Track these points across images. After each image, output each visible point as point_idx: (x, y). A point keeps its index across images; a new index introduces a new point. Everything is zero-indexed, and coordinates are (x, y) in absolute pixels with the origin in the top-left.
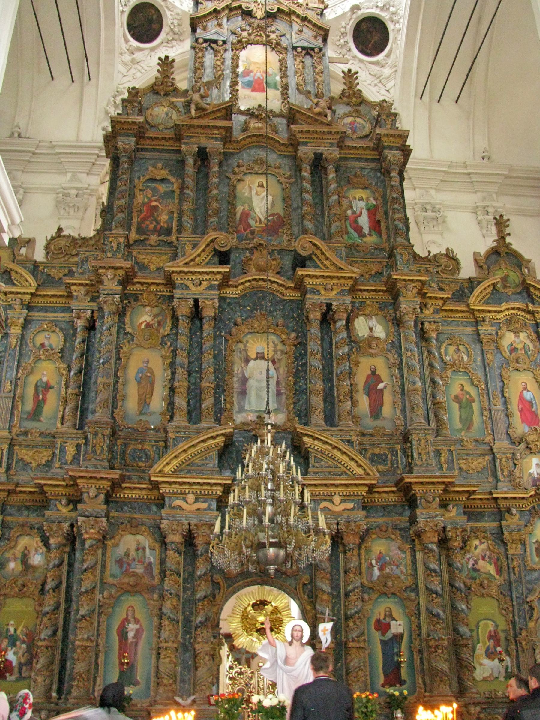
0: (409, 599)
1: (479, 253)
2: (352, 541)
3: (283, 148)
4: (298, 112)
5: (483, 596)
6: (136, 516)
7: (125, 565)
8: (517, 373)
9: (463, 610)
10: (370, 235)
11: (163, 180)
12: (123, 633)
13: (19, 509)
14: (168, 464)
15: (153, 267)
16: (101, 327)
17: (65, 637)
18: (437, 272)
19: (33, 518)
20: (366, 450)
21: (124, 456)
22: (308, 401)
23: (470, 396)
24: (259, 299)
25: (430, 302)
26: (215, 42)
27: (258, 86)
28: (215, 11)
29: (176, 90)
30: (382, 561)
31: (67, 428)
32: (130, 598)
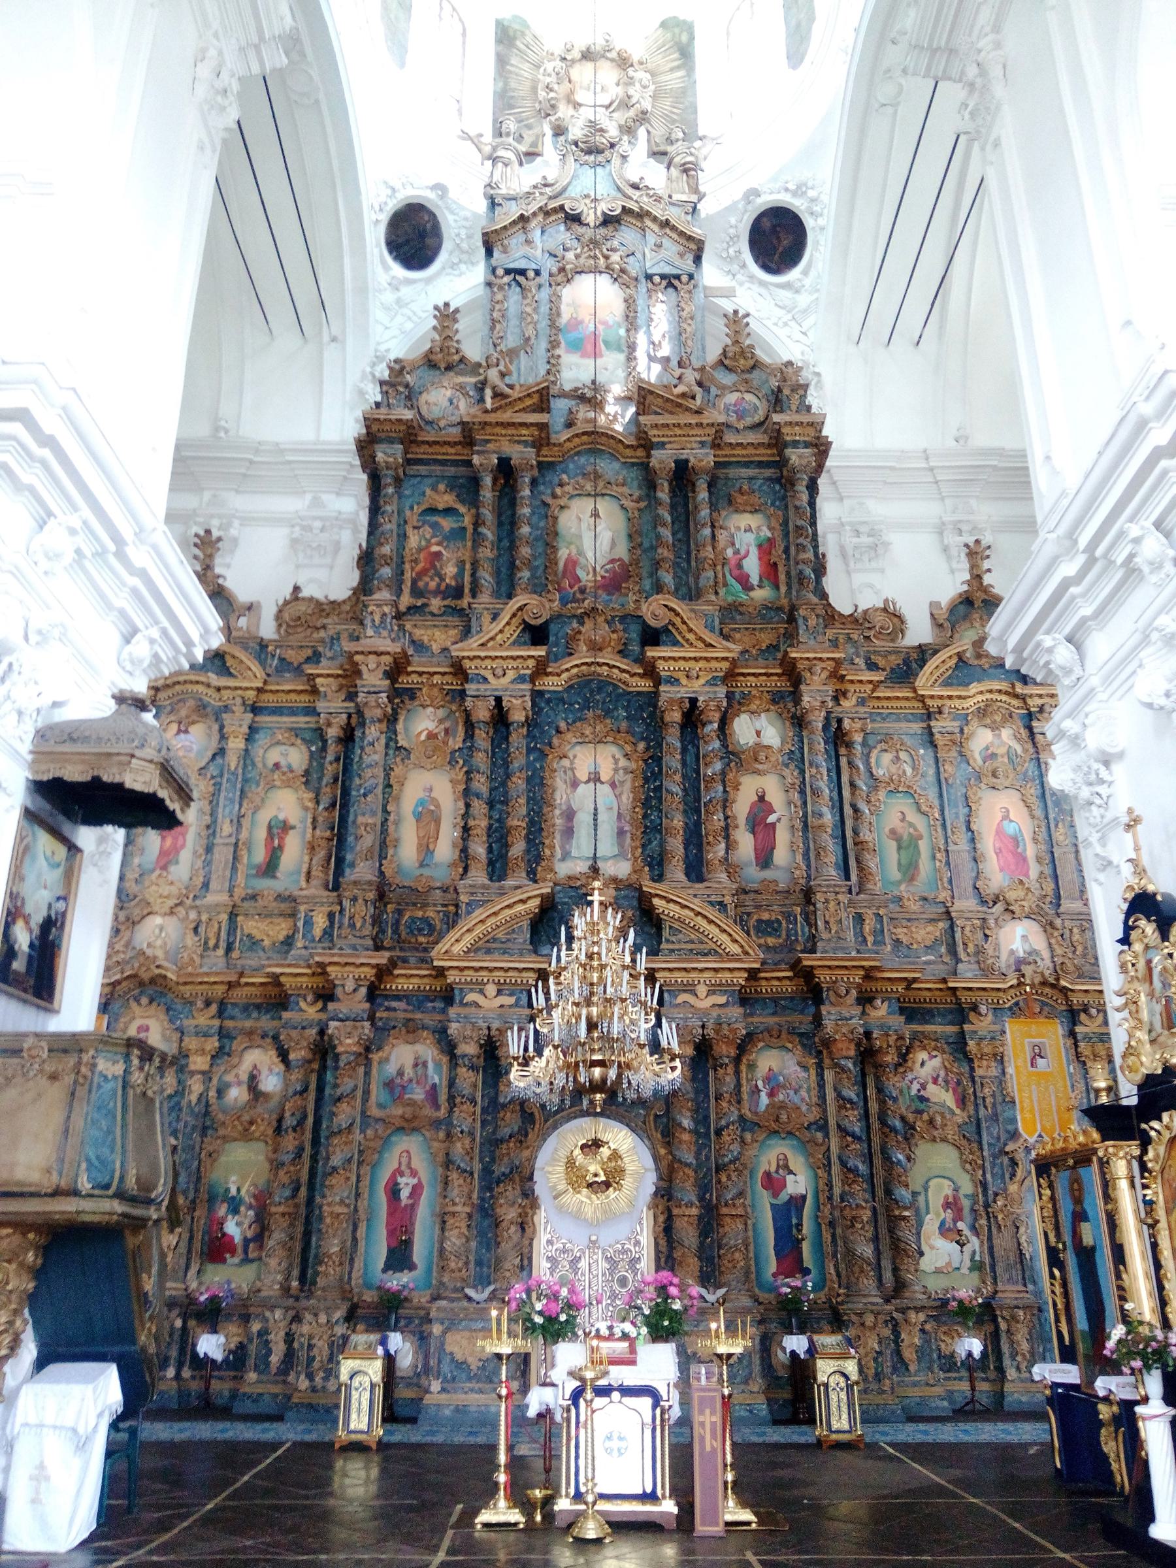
0: (812, 1141)
1: (938, 604)
3: (628, 452)
4: (652, 393)
5: (934, 1140)
7: (397, 1091)
10: (760, 586)
11: (449, 511)
12: (393, 1192)
15: (435, 648)
16: (362, 739)
17: (310, 1201)
19: (266, 1023)
22: (662, 844)
23: (916, 829)
25: (851, 688)
26: (522, 272)
30: (773, 1084)
31: (314, 889)
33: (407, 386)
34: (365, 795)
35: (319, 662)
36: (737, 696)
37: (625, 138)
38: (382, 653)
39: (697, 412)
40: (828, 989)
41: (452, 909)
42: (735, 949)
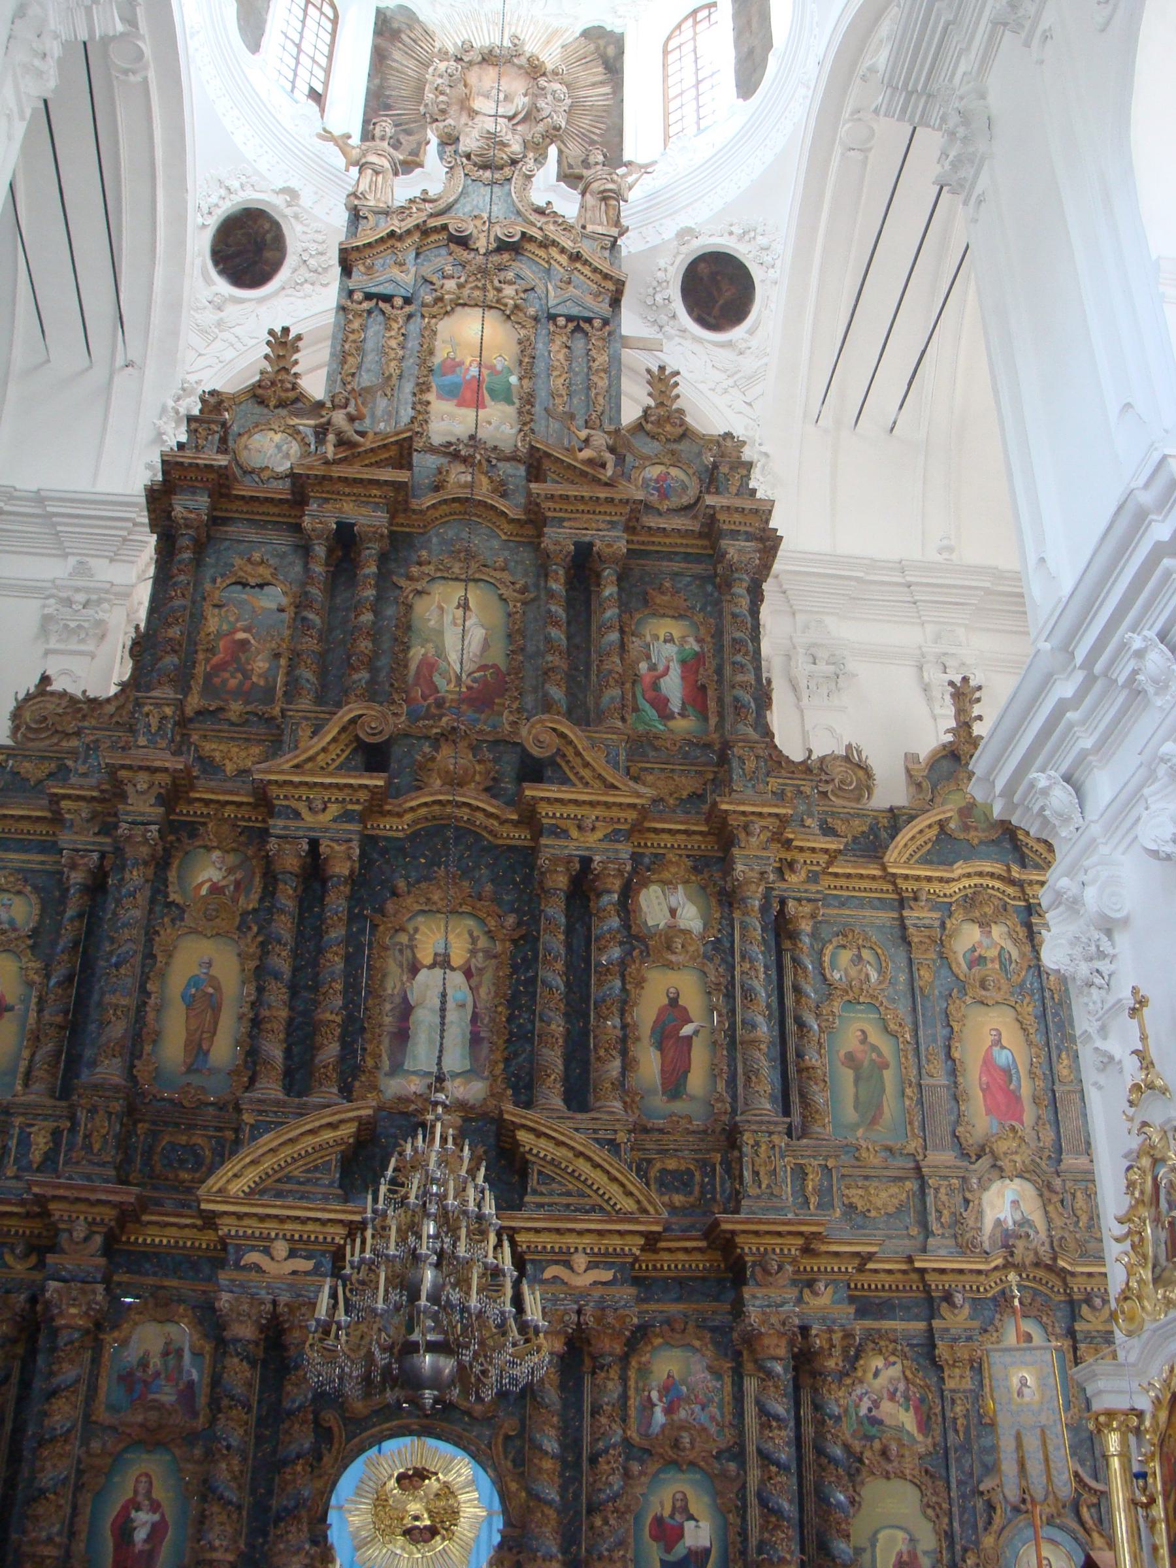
0: (724, 1474)
2: (607, 1348)
7: (139, 1387)
8: (984, 1009)
9: (839, 1503)
10: (683, 715)
20: (649, 1161)
23: (880, 1054)
25: (801, 858)
26: (387, 299)
27: (472, 395)
28: (392, 234)
29: (300, 397)
31: (37, 1094)
33: (224, 424)
34: (117, 966)
35: (66, 779)
36: (647, 860)
37: (531, 155)
38: (155, 770)
39: (606, 484)
40: (754, 1264)
41: (230, 1135)
42: (628, 1205)
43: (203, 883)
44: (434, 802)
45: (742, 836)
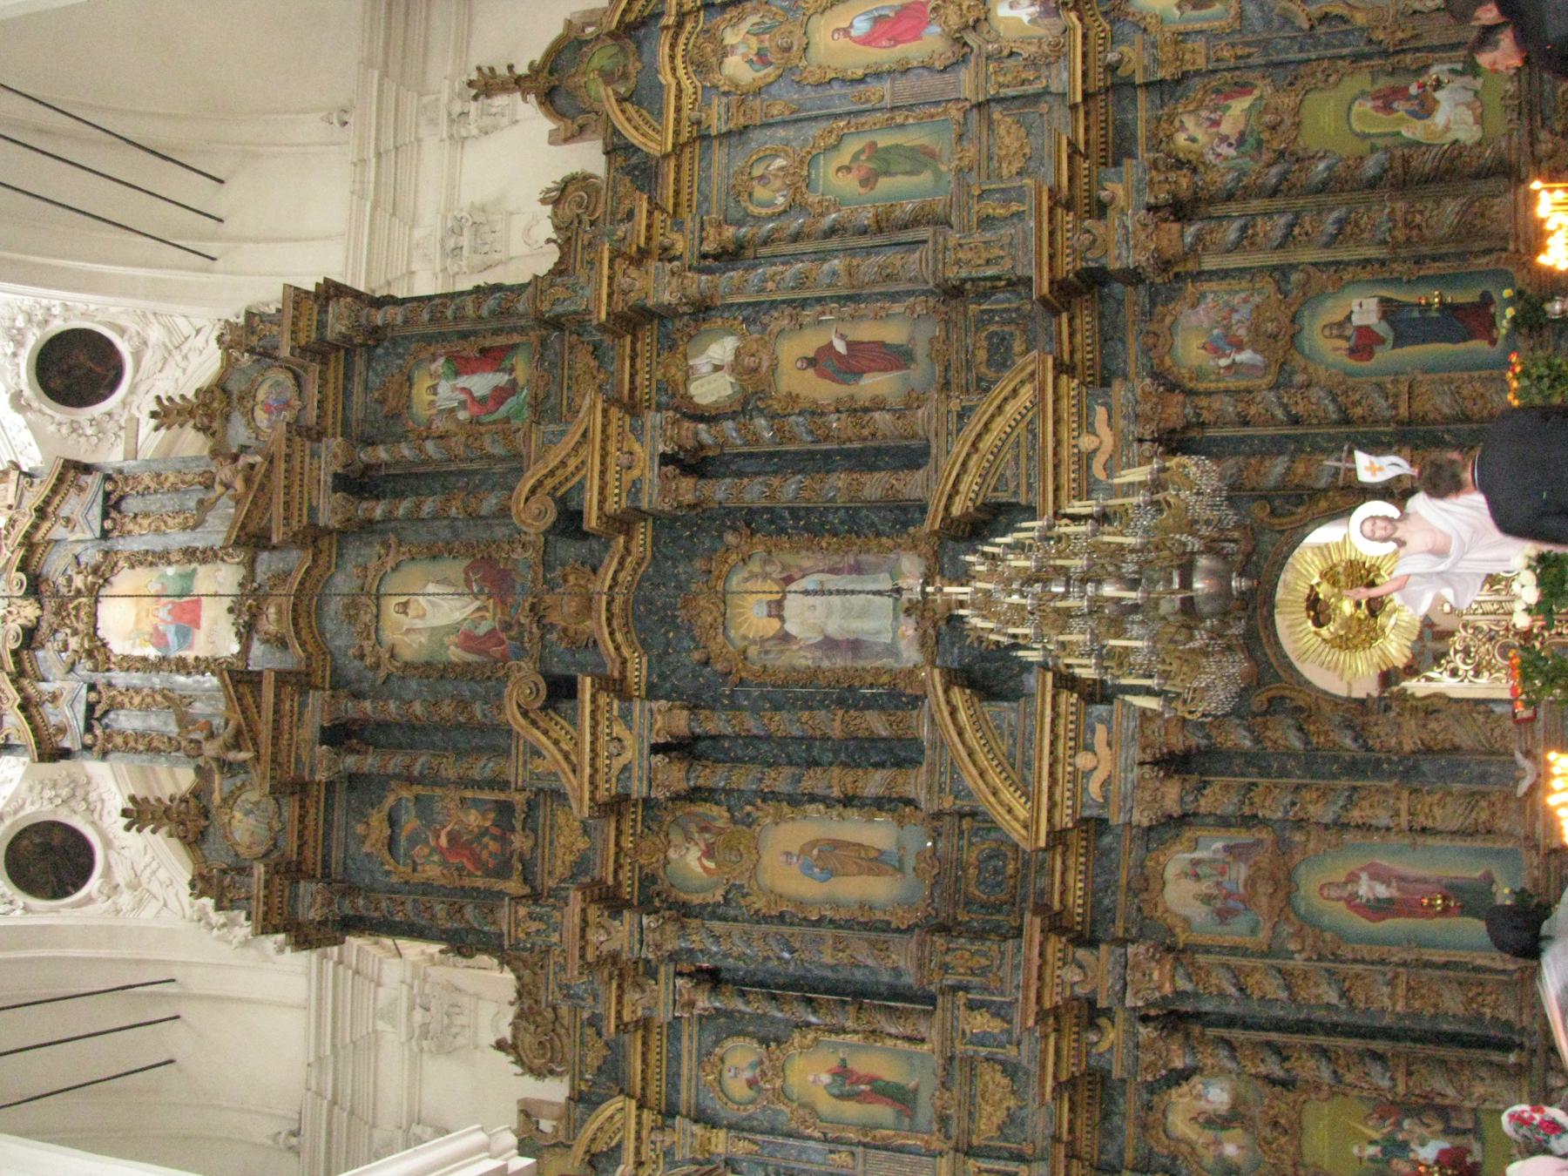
0: (1305, 285)
1: (551, 133)
2: (1177, 410)
4: (243, 526)
5: (1297, 125)
6: (1123, 881)
7: (1231, 903)
8: (812, 50)
9: (1329, 168)
10: (511, 370)
11: (393, 821)
12: (1379, 909)
13: (1110, 1134)
14: (1010, 811)
15: (582, 844)
16: (712, 955)
17: (1387, 1034)
18: (592, 224)
19: (1129, 1104)
20: (980, 379)
21: (993, 906)
22: (873, 506)
23: (862, 151)
24: (650, 612)
26: (91, 708)
27: (187, 614)
28: (23, 707)
29: (196, 793)
31: (931, 1031)
32: (1302, 892)
38: (584, 920)
39: (271, 462)
43: (704, 867)
44: (609, 625)
45: (633, 297)
